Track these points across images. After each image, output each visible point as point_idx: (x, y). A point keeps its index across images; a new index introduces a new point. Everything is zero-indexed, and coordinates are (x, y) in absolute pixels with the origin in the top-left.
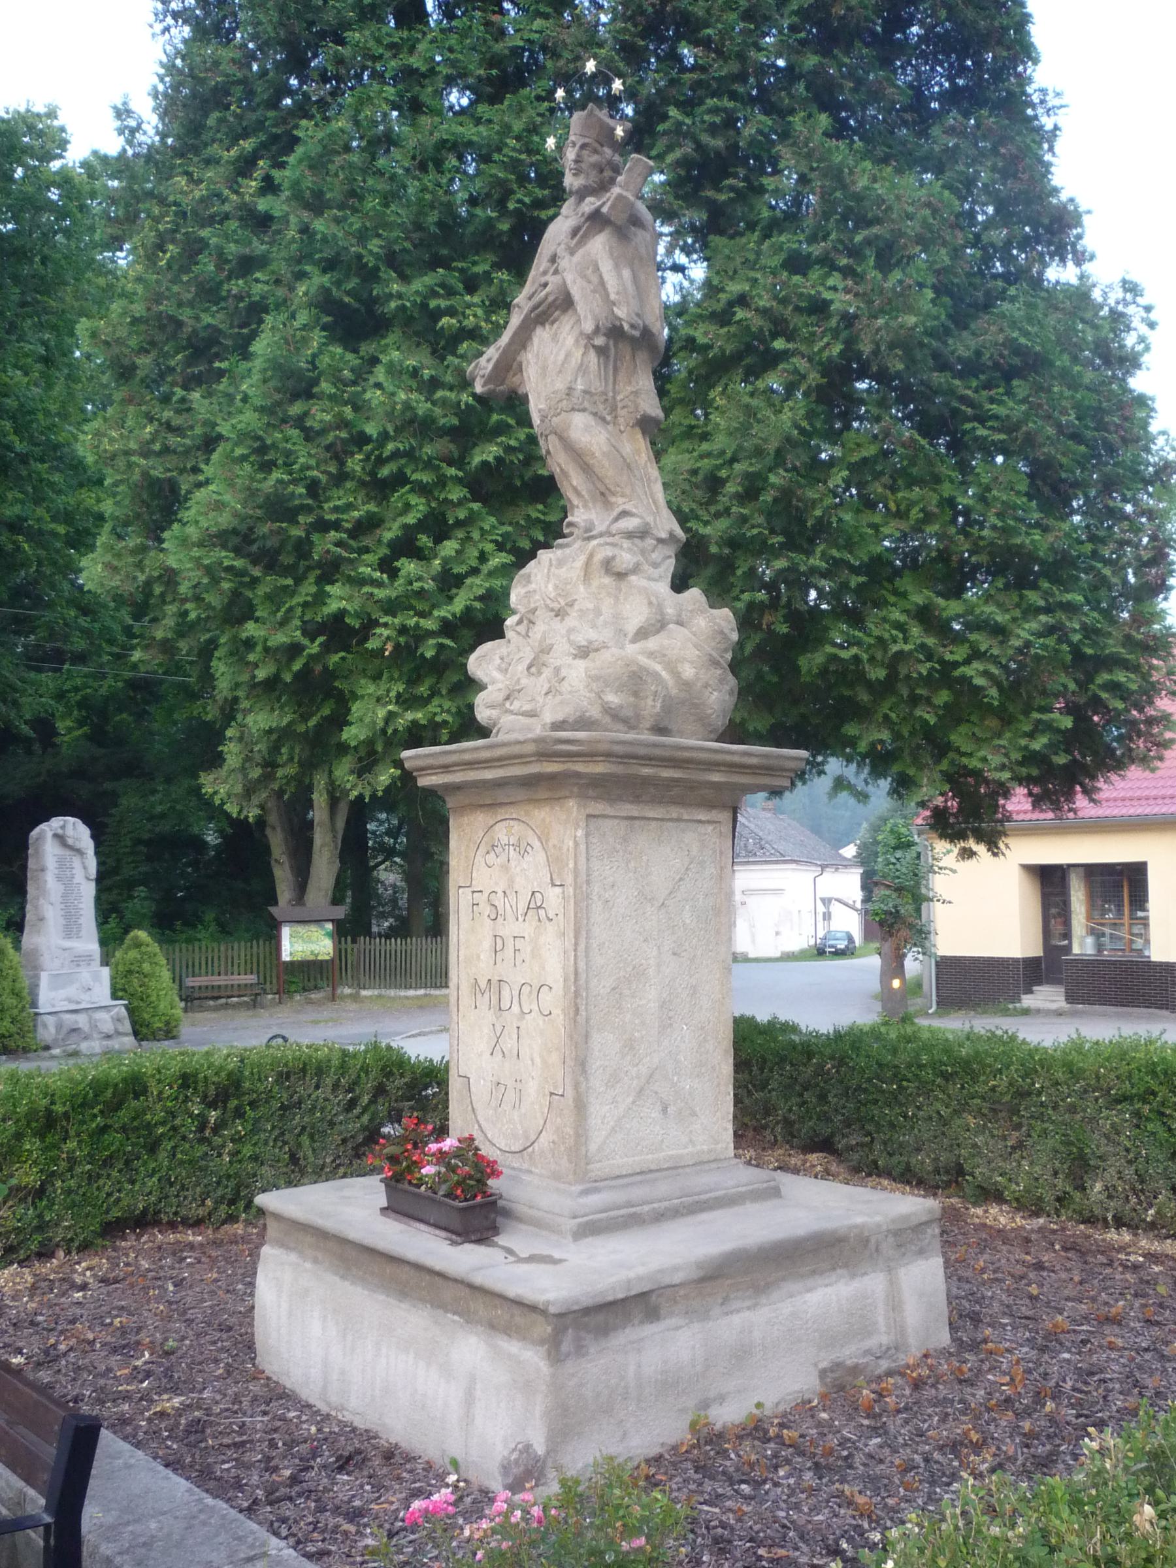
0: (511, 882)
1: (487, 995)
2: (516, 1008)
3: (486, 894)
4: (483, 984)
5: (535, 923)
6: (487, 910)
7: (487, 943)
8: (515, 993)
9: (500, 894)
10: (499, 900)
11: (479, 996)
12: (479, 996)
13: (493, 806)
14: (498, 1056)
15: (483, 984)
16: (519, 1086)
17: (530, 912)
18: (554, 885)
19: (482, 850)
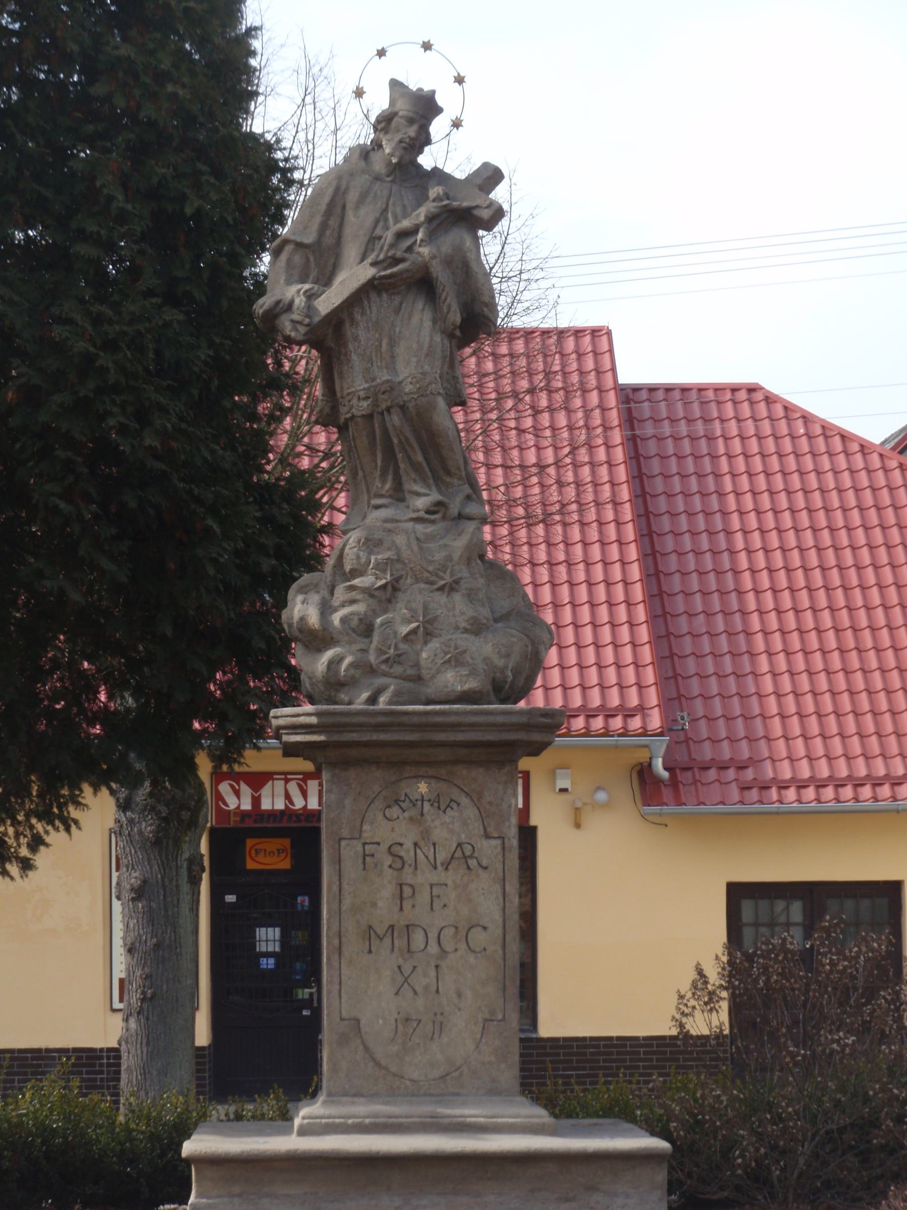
0: (426, 834)
1: (387, 941)
2: (433, 949)
3: (384, 847)
4: (381, 930)
5: (463, 870)
6: (388, 860)
7: (387, 892)
8: (433, 935)
9: (409, 844)
10: (407, 852)
11: (375, 942)
12: (375, 942)
13: (399, 764)
14: (407, 991)
15: (381, 930)
16: (439, 1018)
17: (454, 864)
18: (487, 836)
19: (379, 804)
